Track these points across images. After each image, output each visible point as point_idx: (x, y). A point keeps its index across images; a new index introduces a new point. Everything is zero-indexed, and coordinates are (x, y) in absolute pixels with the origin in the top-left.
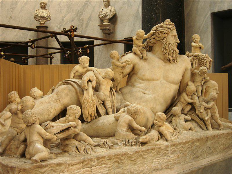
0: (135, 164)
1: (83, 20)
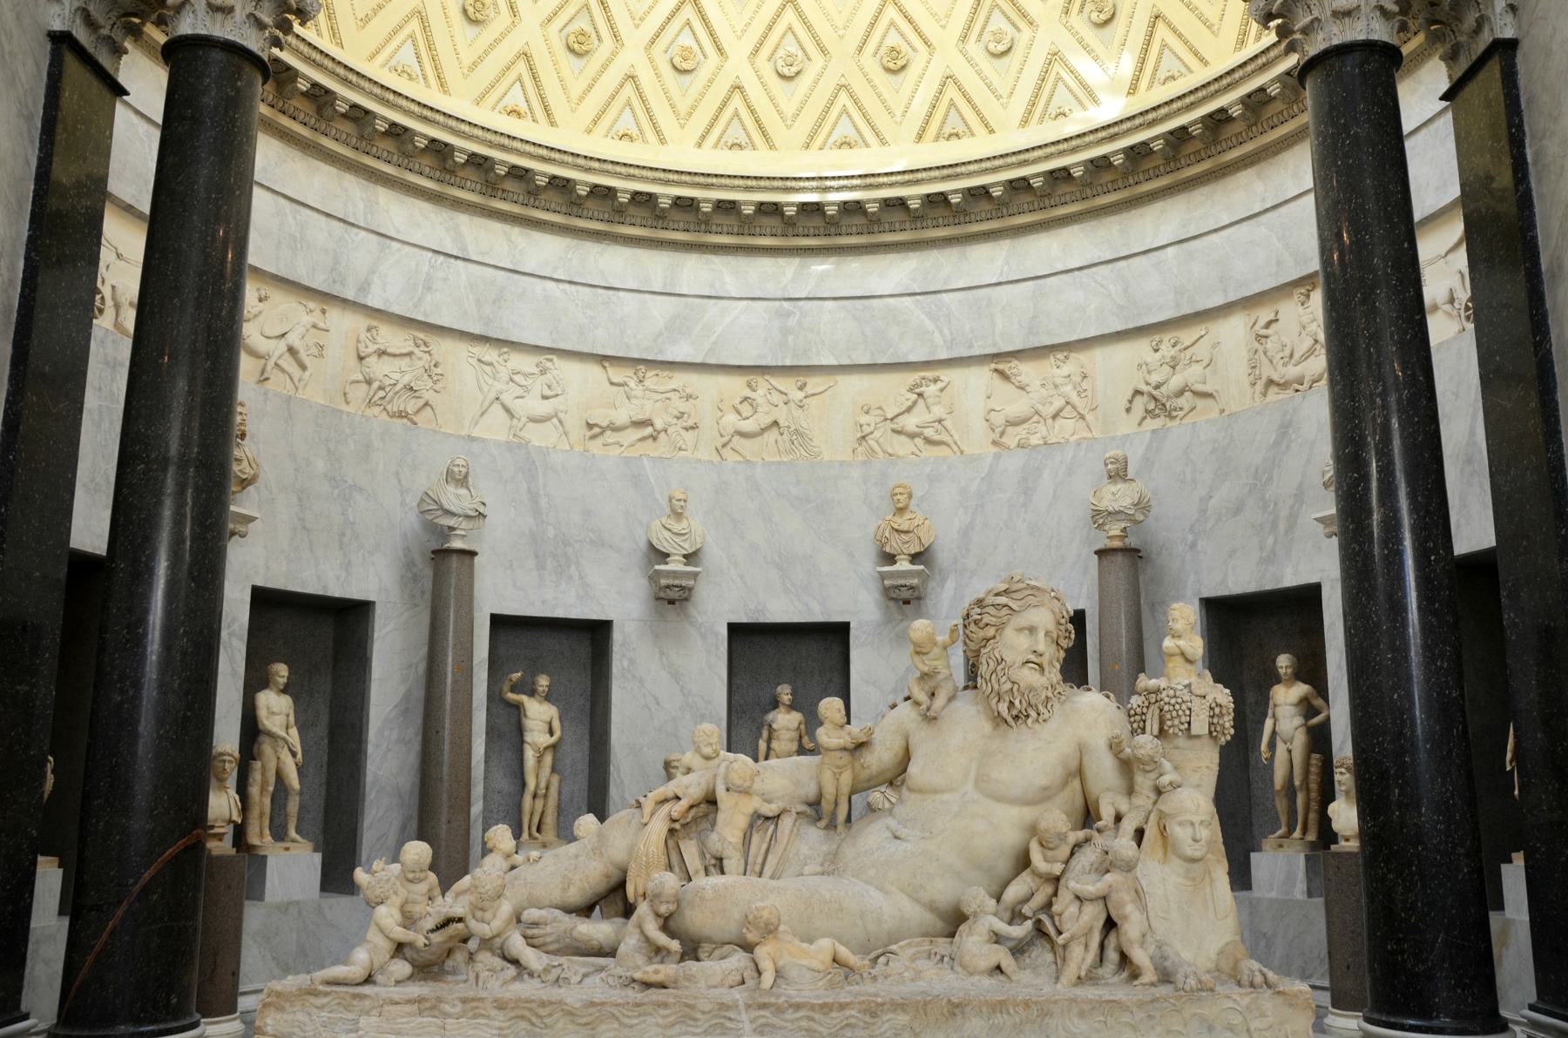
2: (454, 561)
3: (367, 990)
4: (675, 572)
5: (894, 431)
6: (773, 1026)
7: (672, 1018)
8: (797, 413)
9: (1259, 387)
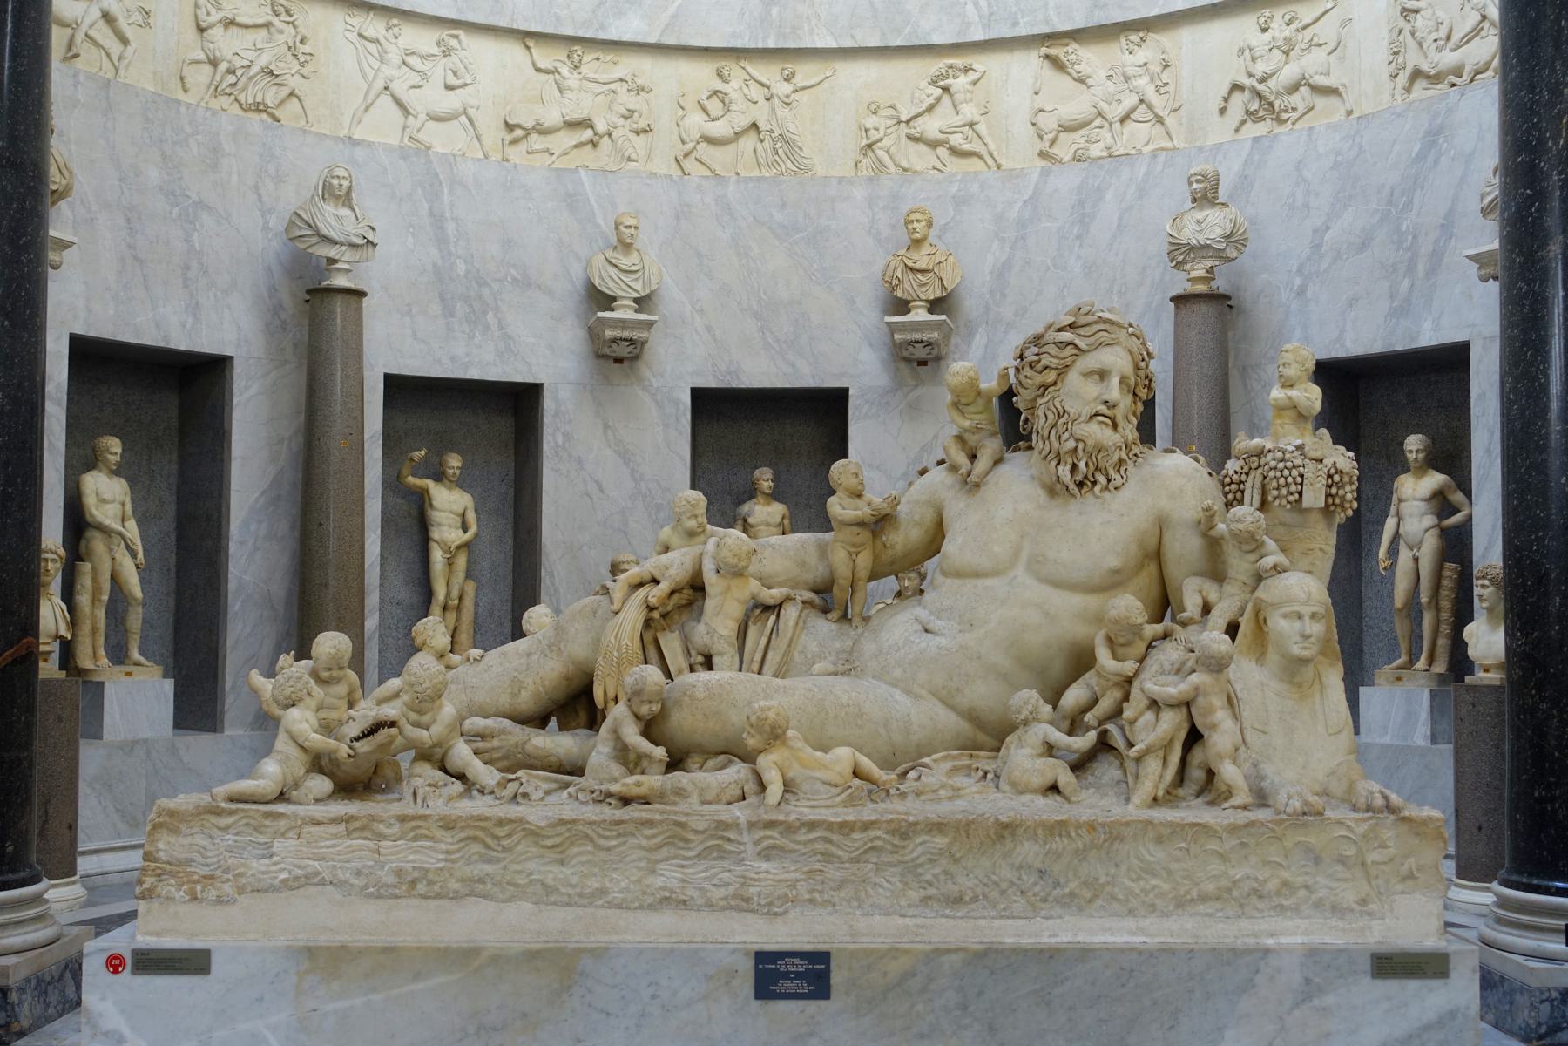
0: (562, 862)
1: (1415, 237)
2: (339, 305)
3: (281, 808)
4: (623, 321)
5: (910, 137)
6: (782, 849)
7: (659, 839)
8: (782, 112)
9: (1403, 79)
